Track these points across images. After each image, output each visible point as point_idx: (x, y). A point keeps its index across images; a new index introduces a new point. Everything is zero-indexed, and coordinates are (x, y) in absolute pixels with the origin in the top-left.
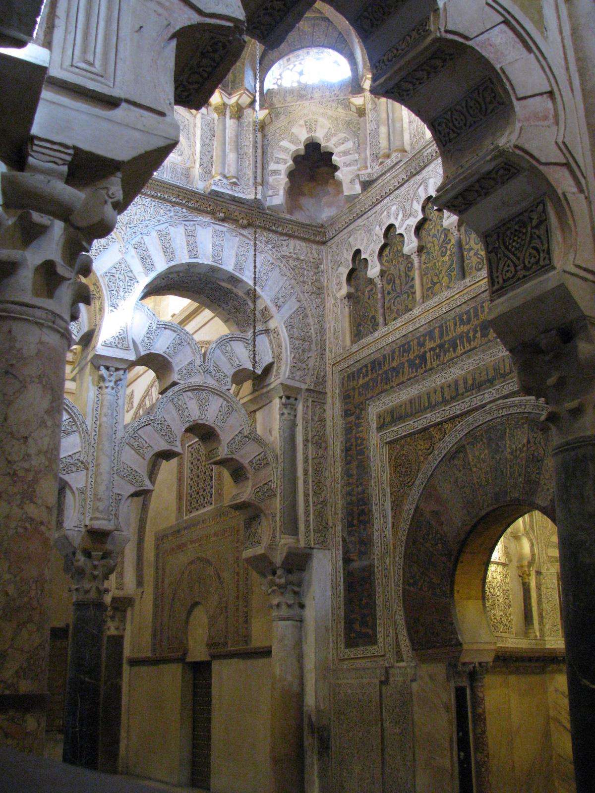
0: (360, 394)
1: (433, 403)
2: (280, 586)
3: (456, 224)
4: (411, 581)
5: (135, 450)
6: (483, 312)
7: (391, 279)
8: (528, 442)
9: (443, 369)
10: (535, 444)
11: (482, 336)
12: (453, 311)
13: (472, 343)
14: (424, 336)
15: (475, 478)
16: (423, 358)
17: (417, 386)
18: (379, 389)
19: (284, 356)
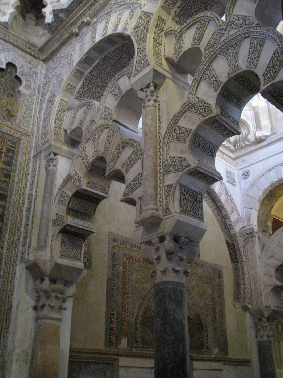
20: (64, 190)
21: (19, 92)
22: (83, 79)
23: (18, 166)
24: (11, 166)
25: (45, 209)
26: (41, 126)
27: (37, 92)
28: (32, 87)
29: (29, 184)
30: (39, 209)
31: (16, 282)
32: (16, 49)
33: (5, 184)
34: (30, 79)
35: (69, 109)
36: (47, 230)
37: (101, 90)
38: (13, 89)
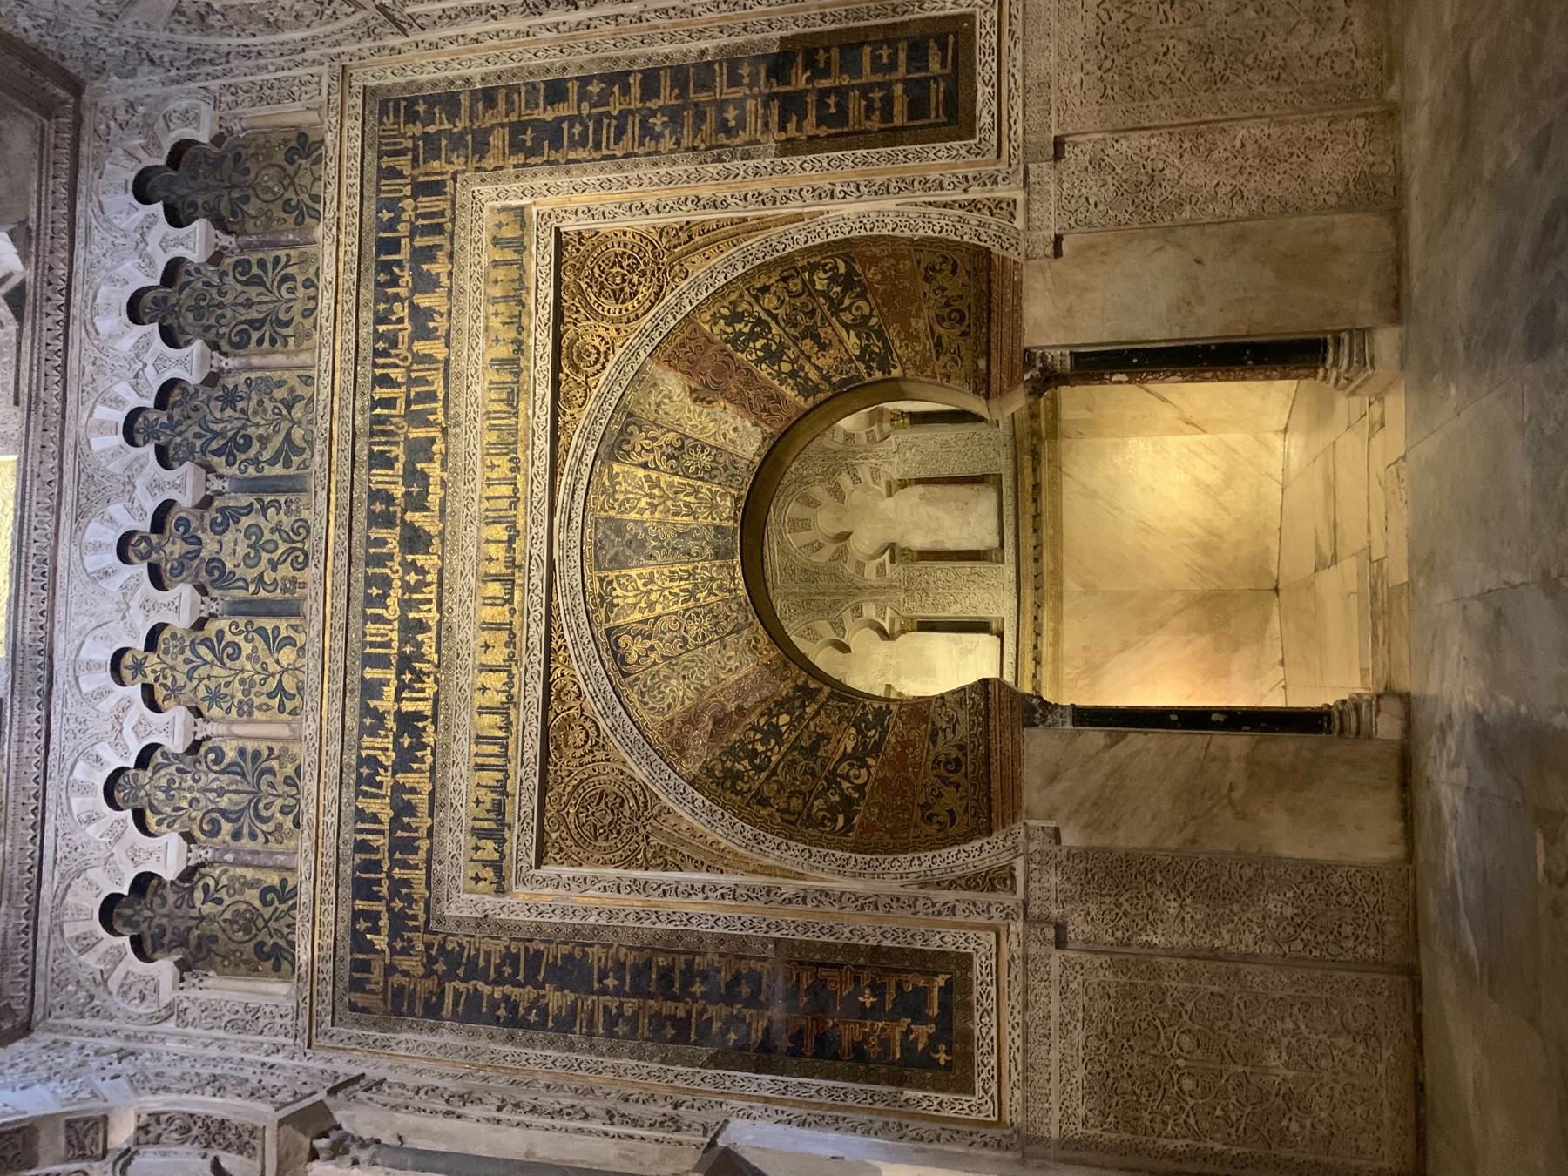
0: (407, 951)
1: (503, 697)
3: (198, 596)
4: (841, 819)
6: (383, 542)
7: (213, 822)
8: (645, 466)
9: (448, 667)
10: (652, 451)
11: (427, 553)
13: (429, 578)
14: (366, 711)
15: (675, 608)
16: (408, 722)
17: (454, 746)
18: (418, 877)
21: (218, 140)
24: (459, 93)
27: (192, 85)
28: (184, 104)
29: (493, 26)
32: (82, 188)
33: (516, 96)
34: (161, 120)
38: (217, 163)
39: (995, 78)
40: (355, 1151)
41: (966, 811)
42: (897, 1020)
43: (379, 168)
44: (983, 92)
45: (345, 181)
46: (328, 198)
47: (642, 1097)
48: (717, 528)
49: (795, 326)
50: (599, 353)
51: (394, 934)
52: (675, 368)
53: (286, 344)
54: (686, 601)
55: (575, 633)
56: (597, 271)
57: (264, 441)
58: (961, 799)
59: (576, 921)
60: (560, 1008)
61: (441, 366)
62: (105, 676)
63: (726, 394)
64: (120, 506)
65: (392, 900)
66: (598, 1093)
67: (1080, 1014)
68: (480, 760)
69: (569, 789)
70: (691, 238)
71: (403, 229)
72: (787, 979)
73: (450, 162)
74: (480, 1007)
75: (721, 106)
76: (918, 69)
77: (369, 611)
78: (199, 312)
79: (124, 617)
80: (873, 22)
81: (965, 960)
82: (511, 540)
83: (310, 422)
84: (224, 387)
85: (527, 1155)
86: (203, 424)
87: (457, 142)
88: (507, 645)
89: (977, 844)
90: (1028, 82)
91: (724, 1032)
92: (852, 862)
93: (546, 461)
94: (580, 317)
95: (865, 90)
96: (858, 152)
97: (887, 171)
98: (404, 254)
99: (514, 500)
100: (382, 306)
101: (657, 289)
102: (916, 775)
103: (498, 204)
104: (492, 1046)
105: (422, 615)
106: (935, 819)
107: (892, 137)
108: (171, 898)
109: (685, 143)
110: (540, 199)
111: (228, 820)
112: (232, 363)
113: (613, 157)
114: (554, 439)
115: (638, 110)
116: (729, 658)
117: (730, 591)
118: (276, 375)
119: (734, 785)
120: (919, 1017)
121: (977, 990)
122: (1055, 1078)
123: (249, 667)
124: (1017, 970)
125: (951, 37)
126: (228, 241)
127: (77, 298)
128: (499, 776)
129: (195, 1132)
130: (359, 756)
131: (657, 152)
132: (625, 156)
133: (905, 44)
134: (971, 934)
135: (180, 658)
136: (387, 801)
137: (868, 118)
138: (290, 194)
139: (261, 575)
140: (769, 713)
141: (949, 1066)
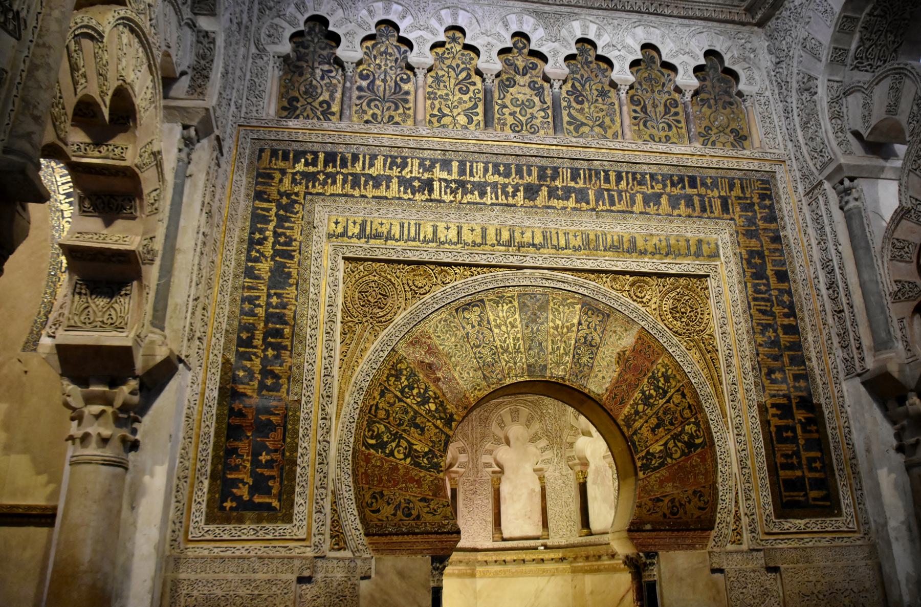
0: (294, 182)
2: (125, 407)
3: (495, 73)
4: (373, 442)
5: (71, 66)
6: (530, 174)
7: (367, 77)
8: (580, 324)
9: (459, 208)
10: (589, 328)
12: (485, 155)
13: (510, 199)
14: (434, 162)
16: (428, 185)
17: (414, 211)
18: (338, 189)
19: (212, 76)
20: (896, 235)
21: (740, 94)
22: (858, 28)
23: (786, 218)
25: (866, 277)
26: (801, 139)
27: (767, 83)
28: (757, 78)
29: (814, 242)
30: (853, 280)
31: (849, 410)
32: (710, 24)
33: (777, 254)
34: (747, 66)
35: (846, 94)
36: (883, 312)
37: (896, 37)
39: (809, 530)
40: (186, 150)
41: (380, 520)
42: (251, 476)
43: (734, 178)
44: (801, 523)
45: (725, 160)
46: (716, 151)
47: (206, 319)
48: (545, 366)
49: (664, 413)
50: (642, 298)
51: (304, 175)
52: (637, 342)
53: (635, 125)
54: (502, 347)
55: (480, 281)
56: (687, 298)
57: (581, 111)
58: (387, 517)
59: (312, 280)
60: (259, 270)
61: (630, 209)
62: (449, 22)
63: (624, 373)
64: (543, 34)
65: (324, 174)
66: (209, 292)
67: (256, 592)
68: (406, 225)
69: (389, 277)
70: (709, 352)
71: (702, 191)
72: (276, 407)
73: (740, 216)
74: (261, 223)
75: (782, 370)
76: (810, 484)
77: (490, 165)
78: (649, 79)
79: (483, 33)
80: (834, 457)
81: (288, 519)
82: (534, 245)
83: (593, 136)
84: (609, 91)
85: (179, 250)
86: (588, 79)
87: (751, 221)
88: (474, 242)
89: (360, 527)
90: (808, 550)
91: (244, 369)
92: (347, 449)
93: (580, 266)
94: (661, 288)
95: (797, 454)
96: (763, 450)
97: (754, 468)
98: (689, 191)
99: (557, 248)
100: (660, 178)
101: (680, 332)
102: (401, 489)
103: (720, 243)
104: (237, 230)
105: (489, 194)
106: (374, 501)
107: (773, 469)
108: (325, 53)
109: (760, 349)
110: (724, 268)
111: (369, 85)
112: (623, 96)
113: (750, 308)
114: (592, 271)
115: (776, 323)
116: (468, 373)
117: (508, 374)
118: (618, 119)
119: (392, 375)
120: (253, 490)
121: (270, 526)
122: (216, 576)
123: (455, 98)
124: (283, 553)
125: (828, 503)
126: (688, 96)
127: (653, 18)
128: (397, 236)
129: (202, 62)
130: (407, 158)
131: (754, 333)
132: (751, 315)
133: (823, 477)
134: (305, 523)
135: (459, 62)
136: (382, 173)
137: (782, 455)
138: (715, 131)
139: (507, 107)
140: (436, 398)
141: (223, 509)
